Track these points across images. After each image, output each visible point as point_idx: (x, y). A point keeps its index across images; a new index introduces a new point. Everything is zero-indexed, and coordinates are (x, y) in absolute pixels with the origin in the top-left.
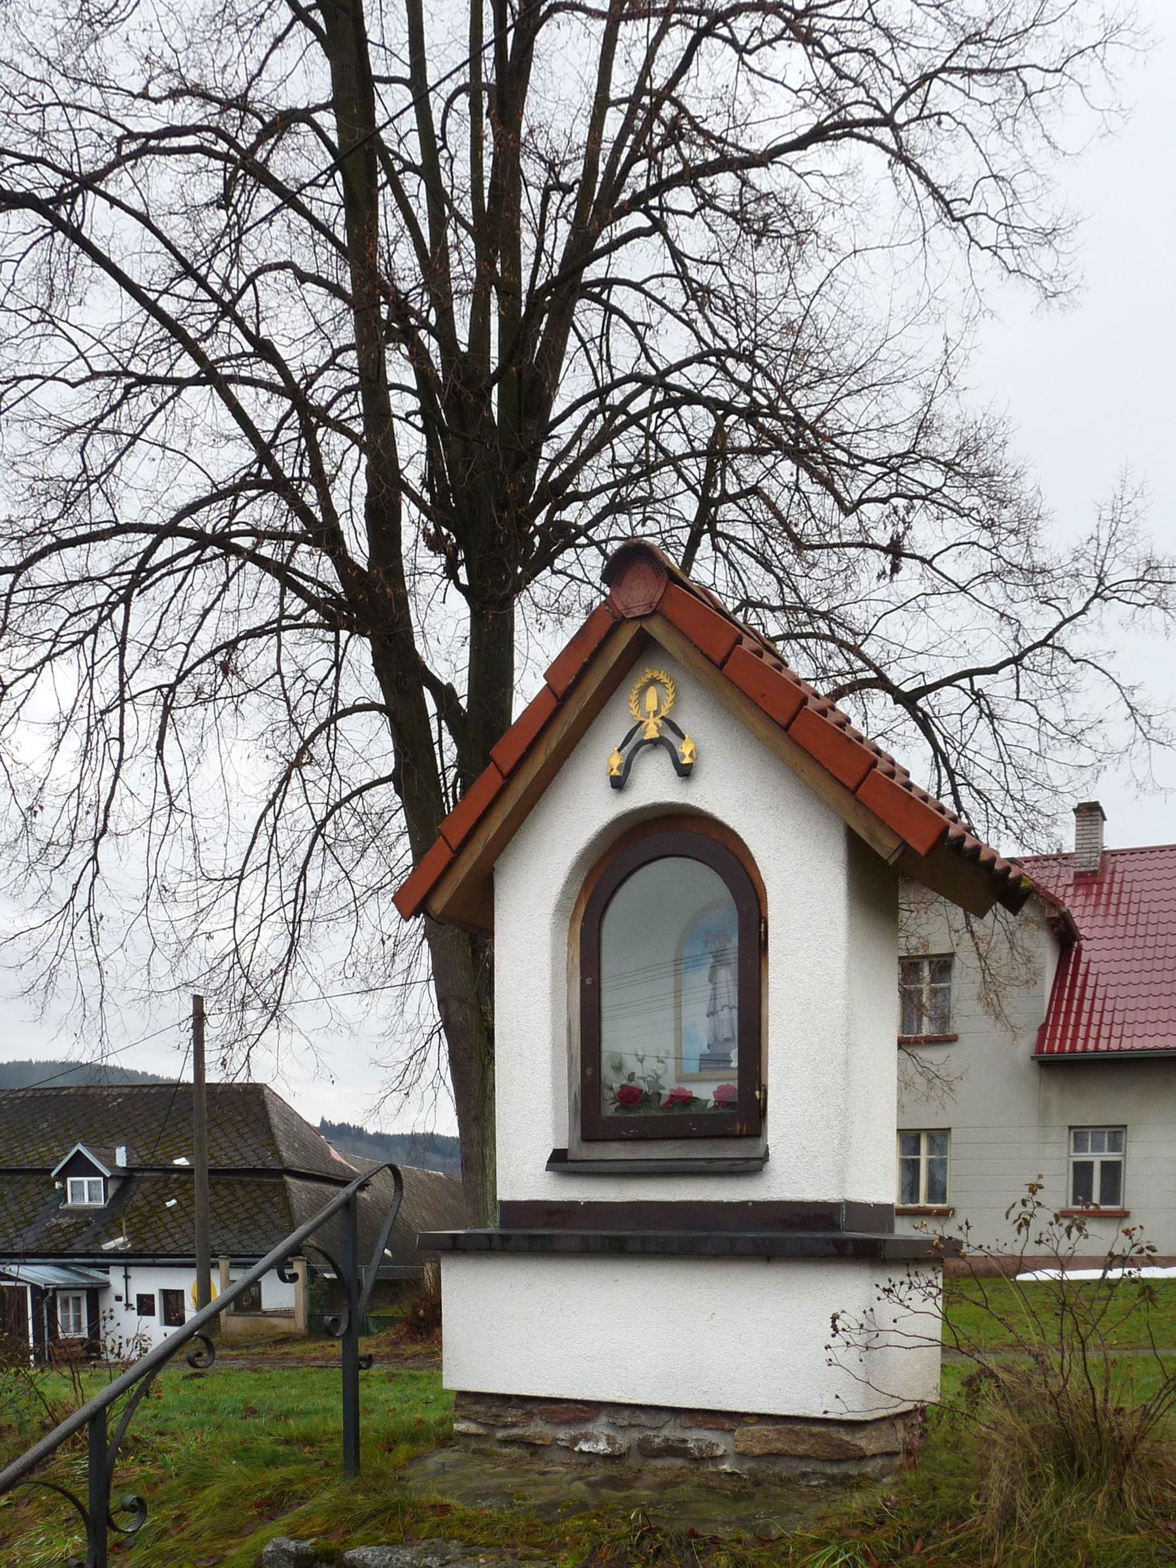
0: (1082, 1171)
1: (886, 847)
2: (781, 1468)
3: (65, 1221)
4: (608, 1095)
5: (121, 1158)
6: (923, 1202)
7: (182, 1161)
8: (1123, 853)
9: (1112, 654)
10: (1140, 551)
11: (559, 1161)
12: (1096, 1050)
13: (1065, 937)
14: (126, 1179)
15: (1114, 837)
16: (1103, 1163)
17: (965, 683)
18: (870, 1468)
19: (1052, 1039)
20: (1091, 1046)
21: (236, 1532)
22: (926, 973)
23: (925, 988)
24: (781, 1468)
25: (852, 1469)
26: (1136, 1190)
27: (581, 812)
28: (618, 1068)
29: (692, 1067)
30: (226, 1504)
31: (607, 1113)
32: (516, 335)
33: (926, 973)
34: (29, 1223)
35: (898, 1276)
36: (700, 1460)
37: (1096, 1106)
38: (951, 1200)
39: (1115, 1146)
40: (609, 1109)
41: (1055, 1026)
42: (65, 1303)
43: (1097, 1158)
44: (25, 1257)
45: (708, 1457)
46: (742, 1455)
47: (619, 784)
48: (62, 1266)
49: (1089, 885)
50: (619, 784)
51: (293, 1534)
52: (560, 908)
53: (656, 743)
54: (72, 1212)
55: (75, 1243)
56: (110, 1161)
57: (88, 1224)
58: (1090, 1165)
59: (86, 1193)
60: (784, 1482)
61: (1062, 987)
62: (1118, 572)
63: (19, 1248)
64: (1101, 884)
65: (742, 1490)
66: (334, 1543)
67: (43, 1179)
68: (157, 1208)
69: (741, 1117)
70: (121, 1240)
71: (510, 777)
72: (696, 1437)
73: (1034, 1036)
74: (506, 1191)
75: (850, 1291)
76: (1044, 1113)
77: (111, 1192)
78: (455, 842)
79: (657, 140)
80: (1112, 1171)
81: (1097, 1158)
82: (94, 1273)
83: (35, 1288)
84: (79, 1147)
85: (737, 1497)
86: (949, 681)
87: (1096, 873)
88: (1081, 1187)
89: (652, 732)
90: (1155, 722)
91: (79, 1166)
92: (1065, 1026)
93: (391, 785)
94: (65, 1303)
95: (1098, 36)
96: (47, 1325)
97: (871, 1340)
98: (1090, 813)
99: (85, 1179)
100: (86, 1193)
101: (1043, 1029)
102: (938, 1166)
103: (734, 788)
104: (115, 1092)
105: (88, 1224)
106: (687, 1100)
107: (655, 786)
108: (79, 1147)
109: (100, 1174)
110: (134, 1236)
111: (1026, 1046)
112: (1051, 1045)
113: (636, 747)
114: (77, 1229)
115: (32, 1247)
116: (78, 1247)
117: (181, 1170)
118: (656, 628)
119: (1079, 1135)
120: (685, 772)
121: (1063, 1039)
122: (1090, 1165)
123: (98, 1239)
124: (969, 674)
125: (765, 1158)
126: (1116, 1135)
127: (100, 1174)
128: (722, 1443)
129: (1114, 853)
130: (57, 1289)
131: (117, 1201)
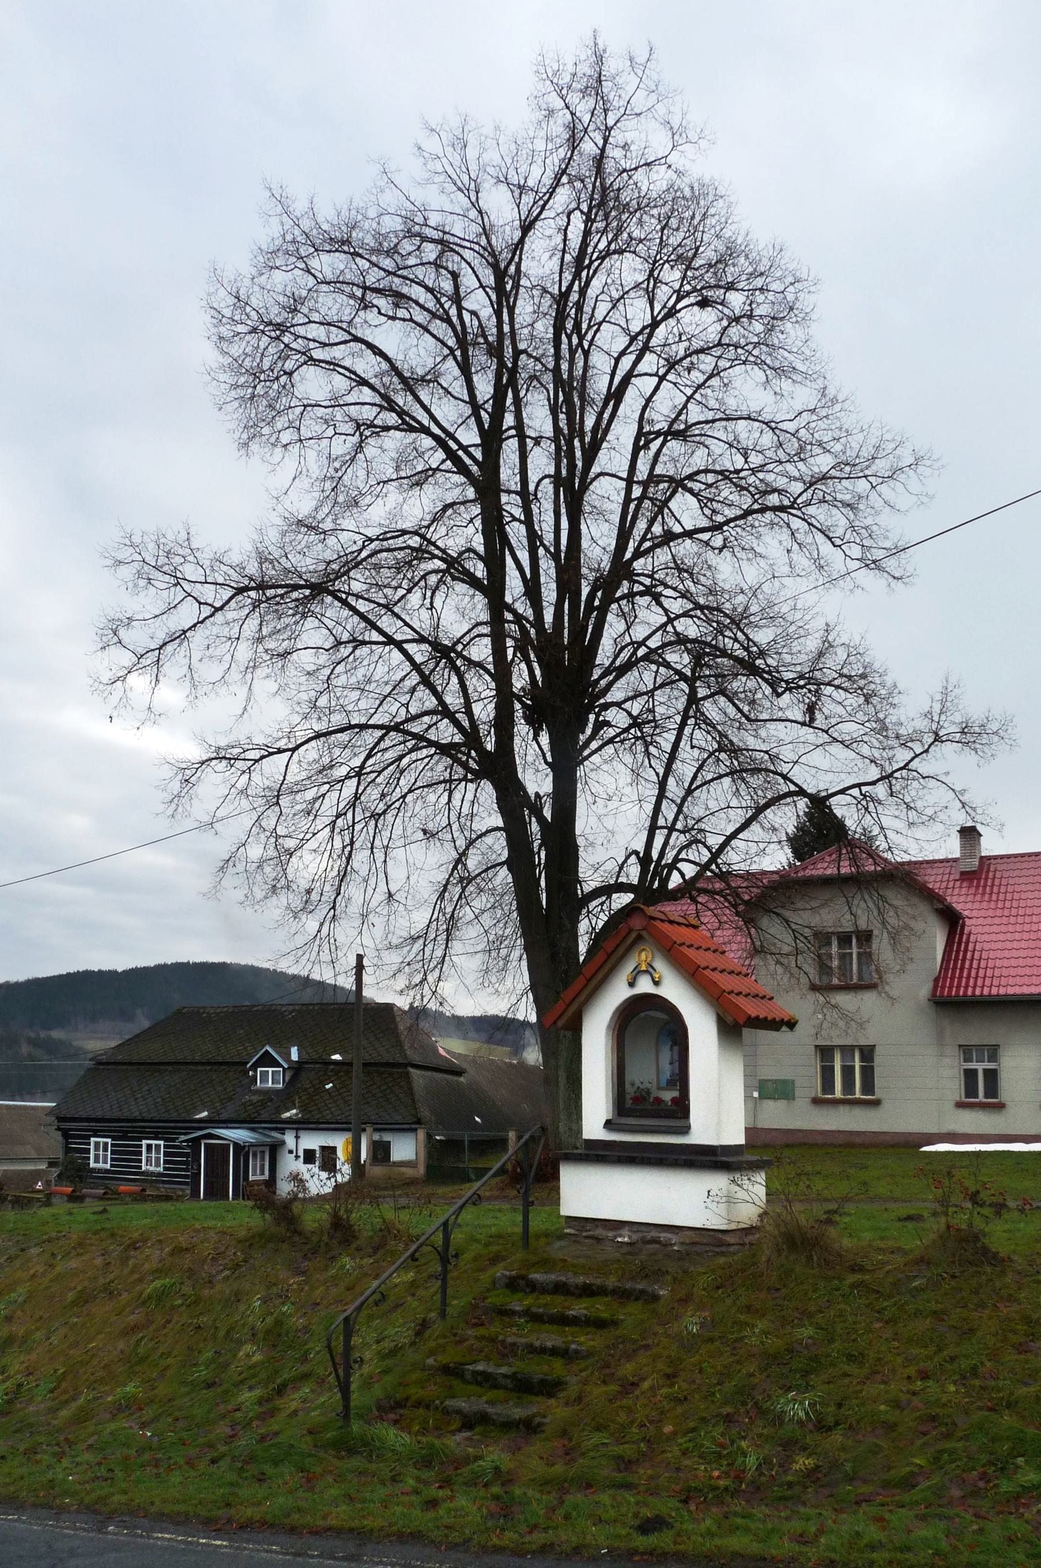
0: (970, 1076)
1: (729, 1019)
2: (698, 1248)
3: (255, 1098)
4: (628, 1097)
5: (294, 1056)
6: (858, 1095)
7: (337, 1057)
8: (995, 857)
9: (947, 774)
10: (957, 718)
11: (608, 1125)
12: (974, 995)
13: (952, 920)
14: (297, 1069)
15: (991, 845)
16: (985, 1071)
17: (855, 792)
18: (732, 1249)
19: (943, 987)
20: (970, 992)
21: (482, 1270)
22: (854, 941)
23: (855, 951)
24: (698, 1248)
25: (724, 1249)
26: (1010, 1087)
27: (617, 993)
28: (633, 1084)
29: (663, 1083)
30: (475, 1259)
31: (628, 1104)
32: (578, 630)
33: (854, 941)
34: (230, 1099)
35: (737, 1176)
36: (665, 1245)
37: (978, 1032)
38: (879, 1094)
39: (994, 1057)
40: (629, 1103)
41: (945, 978)
42: (255, 1155)
43: (980, 1067)
44: (227, 1123)
45: (667, 1244)
46: (682, 1243)
47: (632, 984)
48: (253, 1130)
49: (971, 880)
50: (632, 984)
51: (506, 1269)
52: (609, 1026)
53: (646, 972)
54: (260, 1092)
55: (263, 1114)
56: (287, 1056)
57: (271, 1100)
58: (975, 1071)
59: (270, 1079)
60: (698, 1254)
61: (951, 951)
62: (949, 728)
63: (224, 1116)
64: (979, 879)
65: (680, 1257)
66: (524, 1272)
67: (241, 1068)
68: (320, 1090)
69: (680, 1109)
70: (294, 1111)
71: (589, 980)
72: (664, 1236)
73: (930, 985)
74: (586, 1135)
75: (718, 1182)
76: (940, 1040)
77: (287, 1079)
78: (568, 1001)
79: (661, 486)
80: (992, 1076)
81: (980, 1067)
82: (276, 1135)
83: (236, 1145)
84: (268, 1048)
85: (679, 1259)
86: (842, 792)
87: (979, 872)
88: (971, 1089)
89: (644, 968)
90: (979, 811)
91: (267, 1060)
92: (952, 978)
93: (505, 867)
94: (255, 1155)
95: (912, 460)
96: (242, 1172)
97: (730, 1200)
98: (969, 834)
99: (270, 1070)
100: (270, 1079)
101: (936, 980)
102: (868, 1074)
103: (675, 991)
104: (291, 1008)
105: (271, 1100)
106: (658, 1100)
107: (644, 986)
108: (268, 1048)
109: (280, 1065)
110: (303, 1109)
111: (925, 991)
112: (942, 992)
113: (637, 973)
114: (263, 1104)
115: (234, 1116)
116: (265, 1116)
117: (336, 1063)
118: (644, 933)
119: (967, 1052)
120: (656, 983)
121: (951, 987)
122: (975, 1071)
123: (280, 1110)
124: (859, 785)
125: (689, 1127)
126: (993, 1052)
127: (280, 1065)
128: (674, 1239)
129: (989, 858)
130: (252, 1145)
131: (290, 1084)
